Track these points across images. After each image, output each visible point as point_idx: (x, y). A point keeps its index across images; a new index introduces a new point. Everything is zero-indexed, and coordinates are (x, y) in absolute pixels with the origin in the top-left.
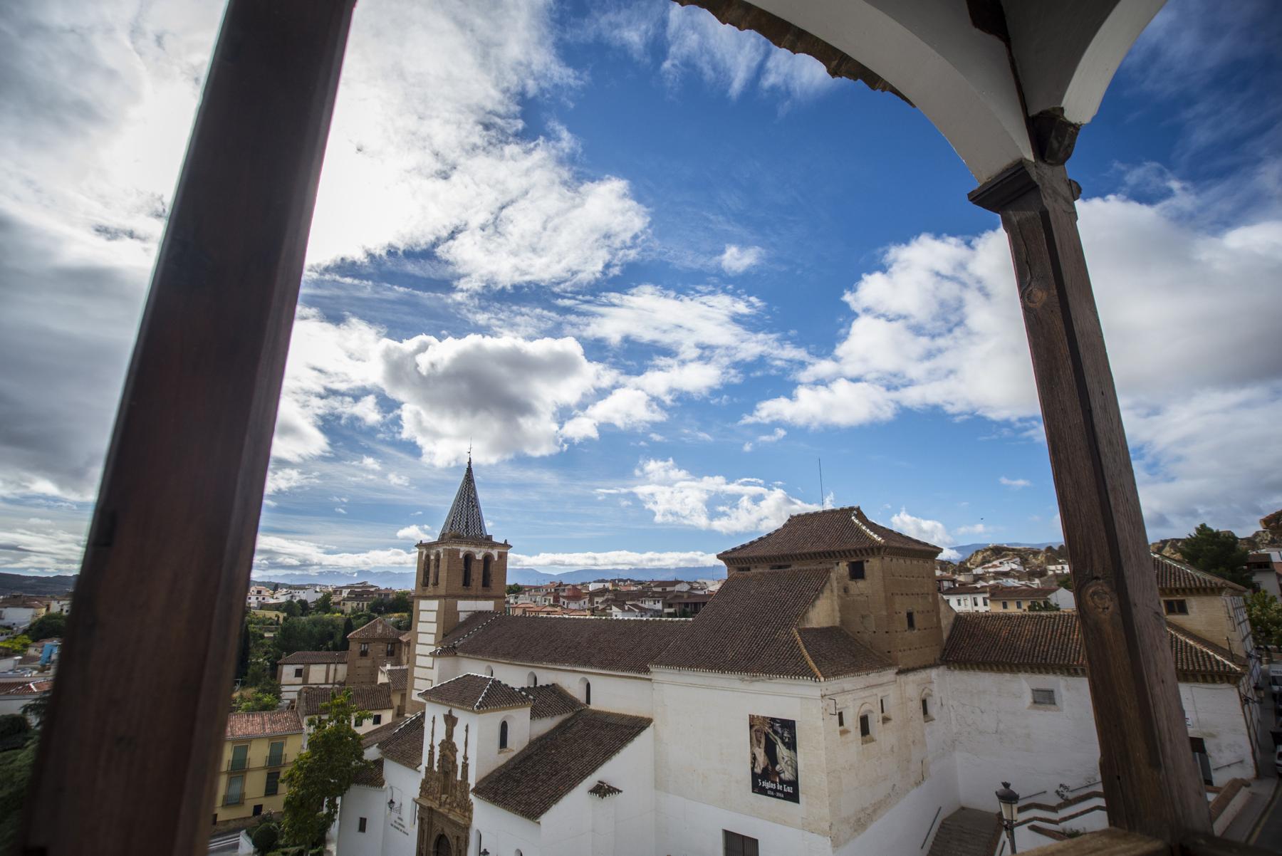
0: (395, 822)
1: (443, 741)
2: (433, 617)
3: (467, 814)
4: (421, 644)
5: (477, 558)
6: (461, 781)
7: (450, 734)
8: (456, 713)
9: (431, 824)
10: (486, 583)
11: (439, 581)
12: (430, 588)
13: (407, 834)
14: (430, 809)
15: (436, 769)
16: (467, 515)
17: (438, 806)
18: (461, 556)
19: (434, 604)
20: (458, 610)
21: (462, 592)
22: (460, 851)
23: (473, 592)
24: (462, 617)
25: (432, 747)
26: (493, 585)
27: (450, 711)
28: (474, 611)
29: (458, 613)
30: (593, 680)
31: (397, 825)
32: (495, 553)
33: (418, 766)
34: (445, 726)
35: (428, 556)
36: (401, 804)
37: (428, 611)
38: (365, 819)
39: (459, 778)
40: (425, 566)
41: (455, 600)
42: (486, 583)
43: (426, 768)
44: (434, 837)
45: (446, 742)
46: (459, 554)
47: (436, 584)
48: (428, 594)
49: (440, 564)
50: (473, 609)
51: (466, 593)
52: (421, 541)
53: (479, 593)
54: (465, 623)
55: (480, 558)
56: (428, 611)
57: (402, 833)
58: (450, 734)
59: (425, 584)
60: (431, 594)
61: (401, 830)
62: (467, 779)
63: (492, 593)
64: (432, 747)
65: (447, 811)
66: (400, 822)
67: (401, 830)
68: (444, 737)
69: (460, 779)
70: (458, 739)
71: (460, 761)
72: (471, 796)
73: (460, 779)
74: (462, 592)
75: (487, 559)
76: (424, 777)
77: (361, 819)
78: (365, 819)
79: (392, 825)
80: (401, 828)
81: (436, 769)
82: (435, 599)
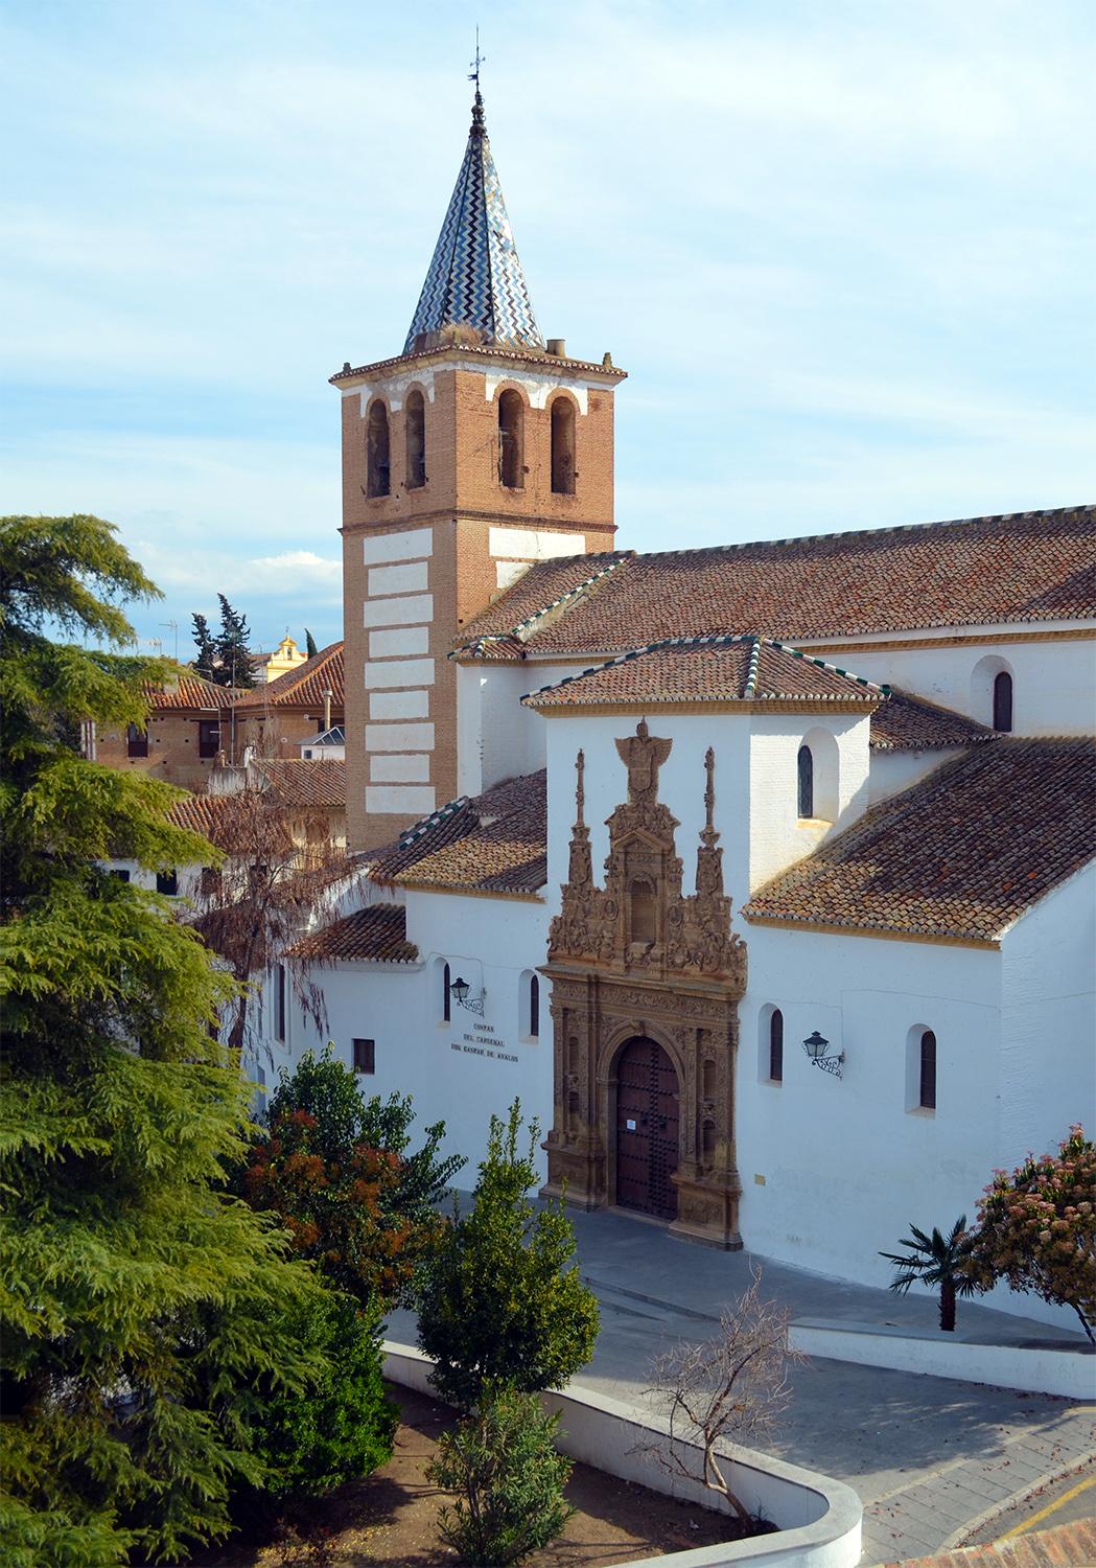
0: (467, 1037)
1: (621, 810)
3: (727, 972)
4: (382, 660)
5: (534, 405)
6: (697, 899)
7: (643, 788)
8: (658, 727)
9: (596, 1019)
10: (562, 480)
11: (428, 472)
12: (399, 499)
13: (515, 1059)
14: (595, 983)
15: (599, 880)
17: (621, 970)
20: (492, 553)
21: (498, 502)
22: (709, 1064)
23: (525, 505)
24: (506, 576)
25: (581, 831)
26: (581, 486)
27: (642, 728)
28: (536, 562)
29: (491, 564)
30: (1021, 661)
32: (580, 395)
33: (538, 887)
34: (626, 769)
35: (379, 408)
36: (484, 992)
37: (396, 564)
38: (370, 1044)
39: (689, 888)
40: (369, 436)
41: (480, 524)
42: (562, 480)
43: (565, 888)
44: (610, 1051)
45: (632, 810)
46: (483, 388)
48: (389, 514)
49: (427, 422)
50: (532, 556)
52: (347, 366)
53: (545, 511)
54: (517, 592)
55: (542, 406)
56: (396, 564)
57: (495, 1060)
58: (643, 788)
60: (406, 512)
61: (491, 1054)
62: (719, 886)
63: (575, 513)
64: (581, 831)
65: (658, 975)
67: (491, 1054)
68: (623, 797)
70: (677, 788)
71: (687, 846)
72: (738, 926)
74: (498, 502)
75: (561, 412)
76: (558, 911)
77: (357, 1042)
78: (370, 1044)
79: (457, 1047)
80: (496, 1050)
81: (599, 880)
82: (421, 526)
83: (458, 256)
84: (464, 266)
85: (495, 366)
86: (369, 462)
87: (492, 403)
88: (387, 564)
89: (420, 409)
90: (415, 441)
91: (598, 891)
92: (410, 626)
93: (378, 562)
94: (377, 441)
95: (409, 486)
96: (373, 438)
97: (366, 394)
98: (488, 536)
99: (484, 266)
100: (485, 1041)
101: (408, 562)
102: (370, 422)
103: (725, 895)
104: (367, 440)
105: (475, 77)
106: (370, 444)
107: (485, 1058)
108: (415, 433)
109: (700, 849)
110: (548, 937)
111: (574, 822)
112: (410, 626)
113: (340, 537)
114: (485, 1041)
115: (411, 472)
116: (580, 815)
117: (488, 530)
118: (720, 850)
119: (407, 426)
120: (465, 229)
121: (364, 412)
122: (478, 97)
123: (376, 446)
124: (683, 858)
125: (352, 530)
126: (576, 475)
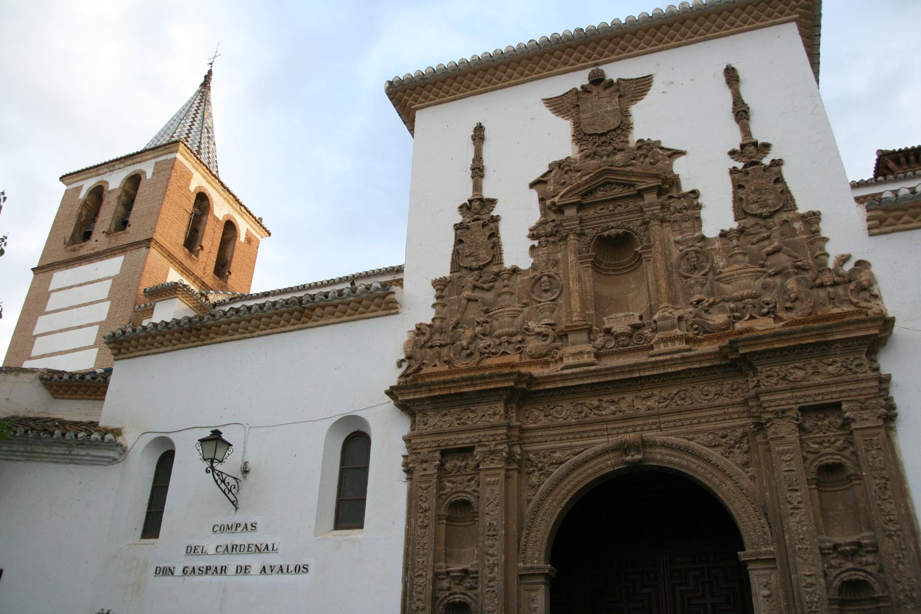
0: (192, 550)
1: (560, 166)
2: (104, 289)
11: (131, 220)
12: (98, 241)
13: (302, 569)
16: (200, 142)
18: (193, 187)
19: (113, 266)
21: (181, 253)
31: (199, 562)
32: (243, 226)
35: (98, 193)
36: (245, 471)
40: (82, 209)
47: (123, 224)
51: (188, 263)
57: (255, 579)
59: (84, 232)
66: (240, 538)
67: (243, 570)
69: (730, 223)
73: (730, 223)
79: (169, 571)
80: (255, 562)
83: (181, 128)
84: (183, 133)
85: (199, 171)
86: (76, 224)
87: (193, 193)
88: (71, 287)
89: (132, 192)
90: (121, 209)
91: (515, 271)
92: (80, 327)
93: (60, 287)
94: (86, 216)
95: (108, 233)
96: (84, 213)
97: (88, 184)
98: (168, 271)
99: (198, 137)
100: (234, 549)
101: (92, 282)
102: (86, 200)
103: (802, 209)
104: (80, 211)
105: (211, 64)
106: (80, 215)
107: (231, 579)
108: (124, 205)
109: (733, 171)
110: (403, 357)
111: (466, 194)
112: (80, 327)
113: (31, 275)
114: (234, 549)
115: (113, 226)
116: (477, 187)
117: (169, 269)
118: (777, 163)
119: (120, 197)
120: (188, 119)
121: (83, 194)
122: (210, 72)
123: (84, 218)
124: (699, 189)
125: (43, 270)
126: (230, 273)
